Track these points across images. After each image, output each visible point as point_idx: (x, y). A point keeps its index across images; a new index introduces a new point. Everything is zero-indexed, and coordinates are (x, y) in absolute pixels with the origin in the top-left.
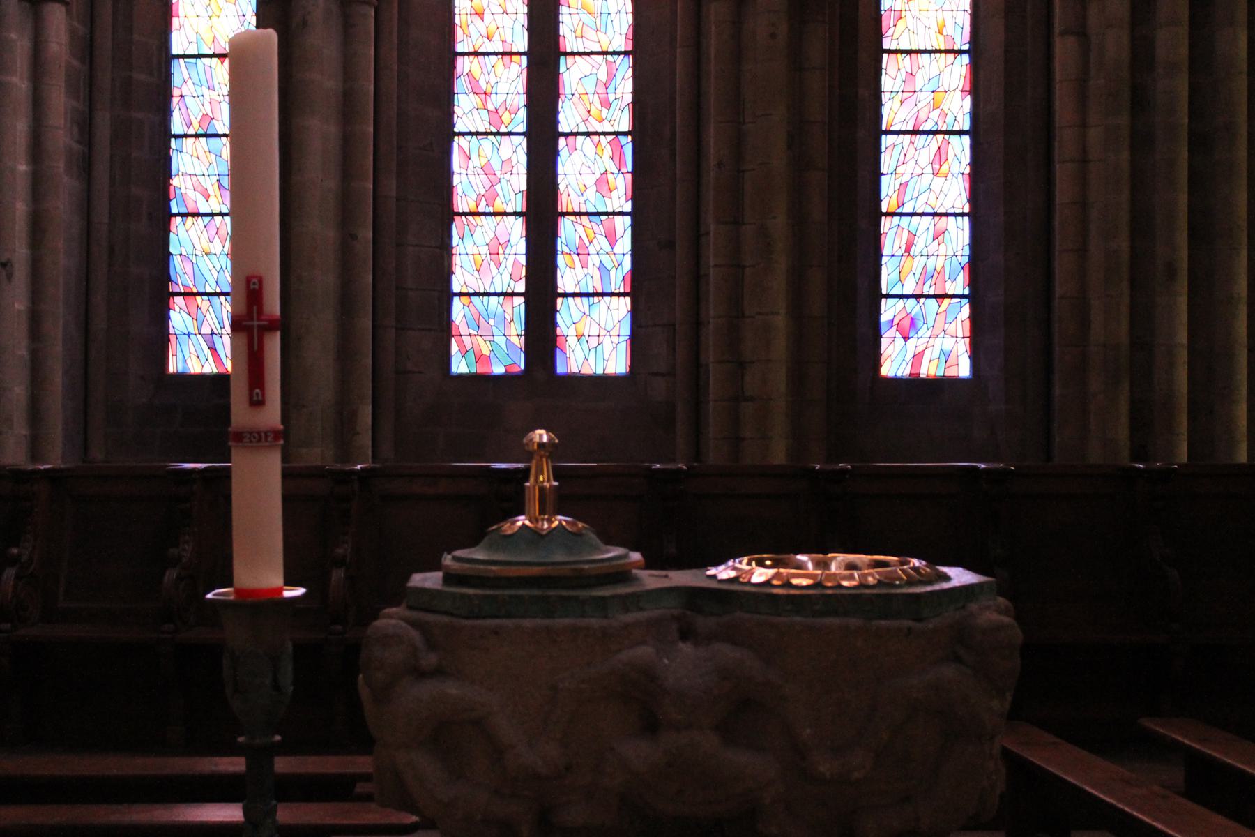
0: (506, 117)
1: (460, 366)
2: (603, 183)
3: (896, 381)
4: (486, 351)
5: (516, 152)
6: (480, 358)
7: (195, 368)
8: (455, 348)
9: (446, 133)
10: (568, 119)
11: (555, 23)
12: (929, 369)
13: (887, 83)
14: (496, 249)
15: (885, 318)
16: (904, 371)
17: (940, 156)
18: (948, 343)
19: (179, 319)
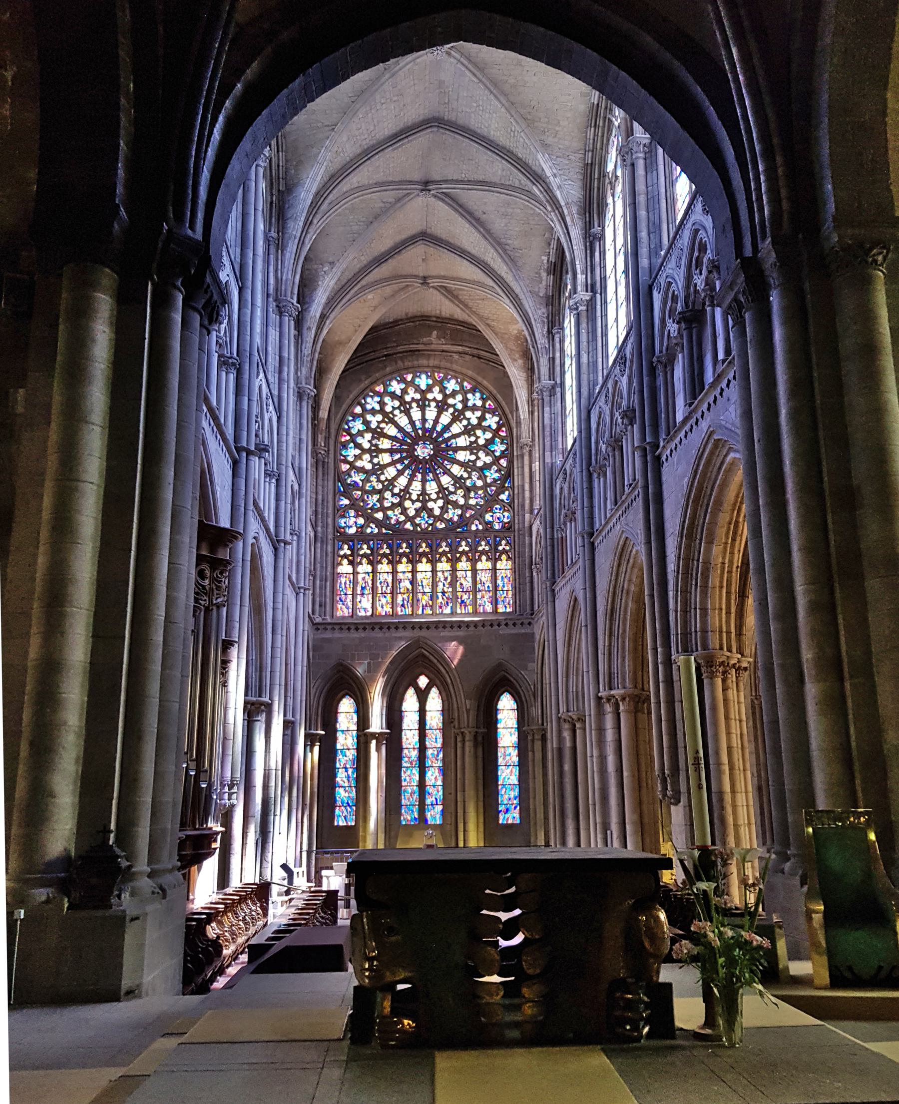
0: (414, 763)
1: (404, 823)
2: (436, 778)
3: (502, 824)
4: (409, 818)
5: (416, 771)
6: (408, 820)
7: (341, 824)
8: (402, 818)
9: (400, 767)
10: (428, 763)
11: (425, 741)
12: (510, 822)
13: (499, 754)
14: (412, 793)
15: (500, 809)
16: (505, 822)
17: (512, 771)
18: (515, 815)
19: (337, 812)
